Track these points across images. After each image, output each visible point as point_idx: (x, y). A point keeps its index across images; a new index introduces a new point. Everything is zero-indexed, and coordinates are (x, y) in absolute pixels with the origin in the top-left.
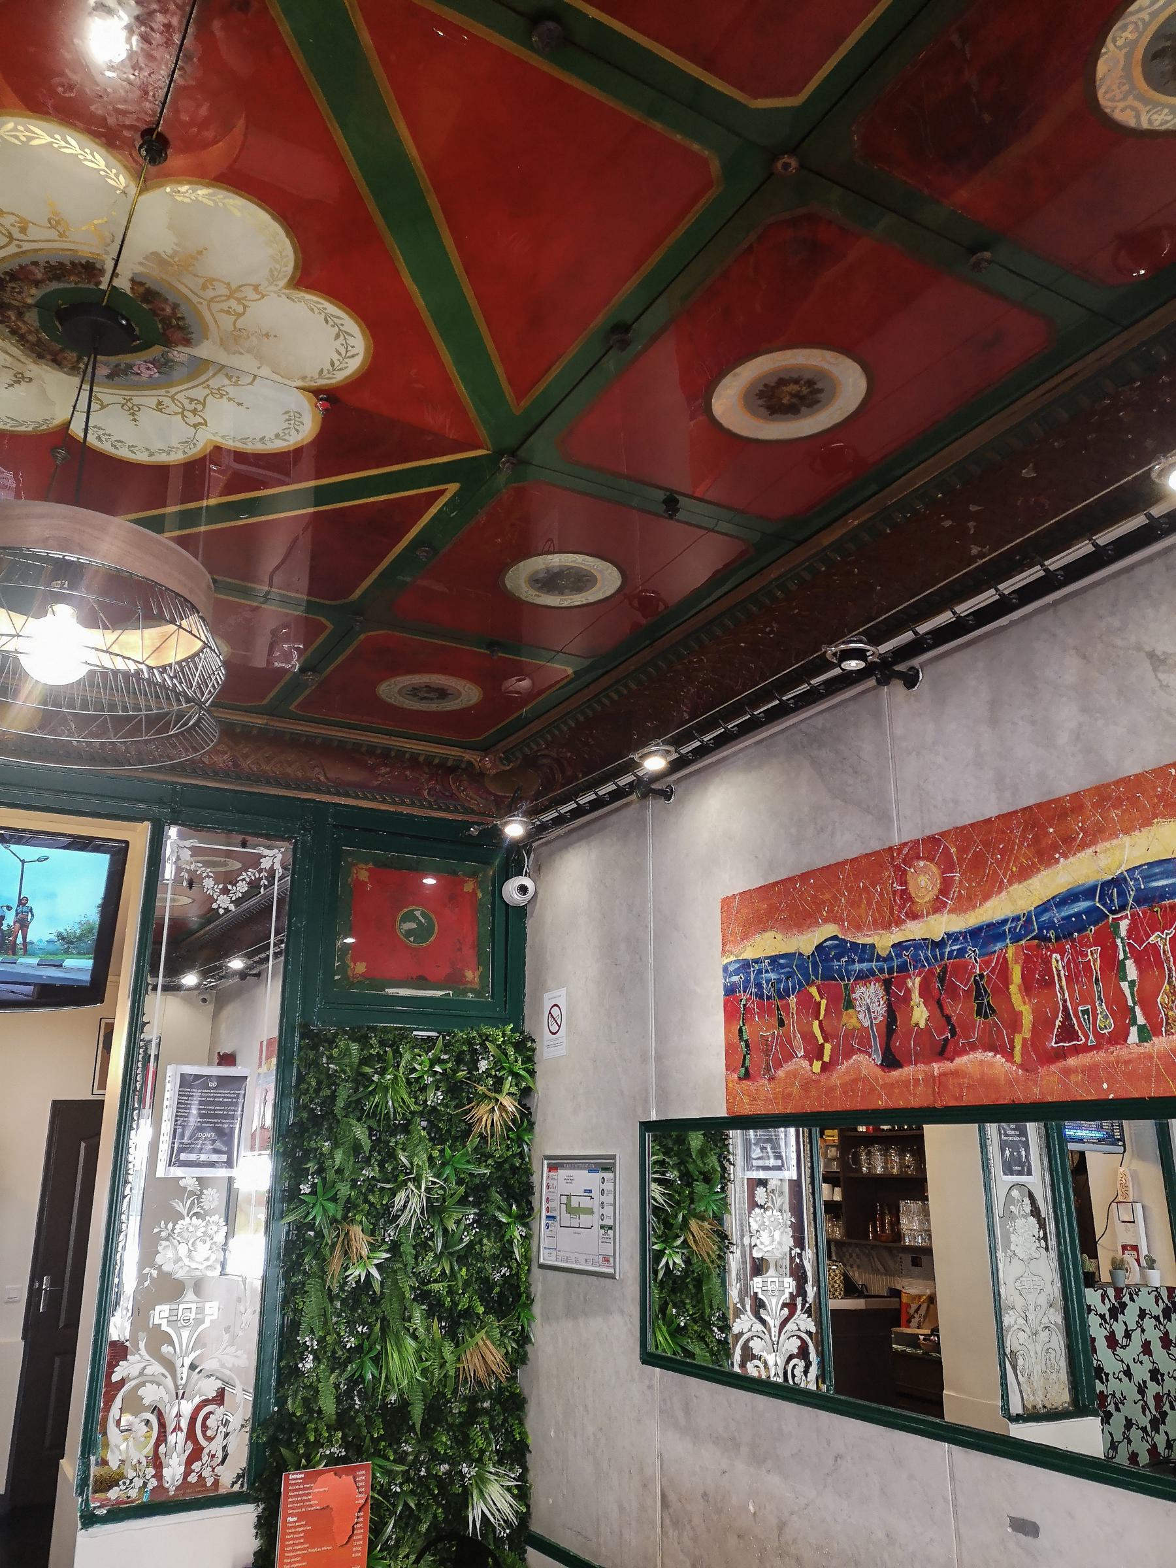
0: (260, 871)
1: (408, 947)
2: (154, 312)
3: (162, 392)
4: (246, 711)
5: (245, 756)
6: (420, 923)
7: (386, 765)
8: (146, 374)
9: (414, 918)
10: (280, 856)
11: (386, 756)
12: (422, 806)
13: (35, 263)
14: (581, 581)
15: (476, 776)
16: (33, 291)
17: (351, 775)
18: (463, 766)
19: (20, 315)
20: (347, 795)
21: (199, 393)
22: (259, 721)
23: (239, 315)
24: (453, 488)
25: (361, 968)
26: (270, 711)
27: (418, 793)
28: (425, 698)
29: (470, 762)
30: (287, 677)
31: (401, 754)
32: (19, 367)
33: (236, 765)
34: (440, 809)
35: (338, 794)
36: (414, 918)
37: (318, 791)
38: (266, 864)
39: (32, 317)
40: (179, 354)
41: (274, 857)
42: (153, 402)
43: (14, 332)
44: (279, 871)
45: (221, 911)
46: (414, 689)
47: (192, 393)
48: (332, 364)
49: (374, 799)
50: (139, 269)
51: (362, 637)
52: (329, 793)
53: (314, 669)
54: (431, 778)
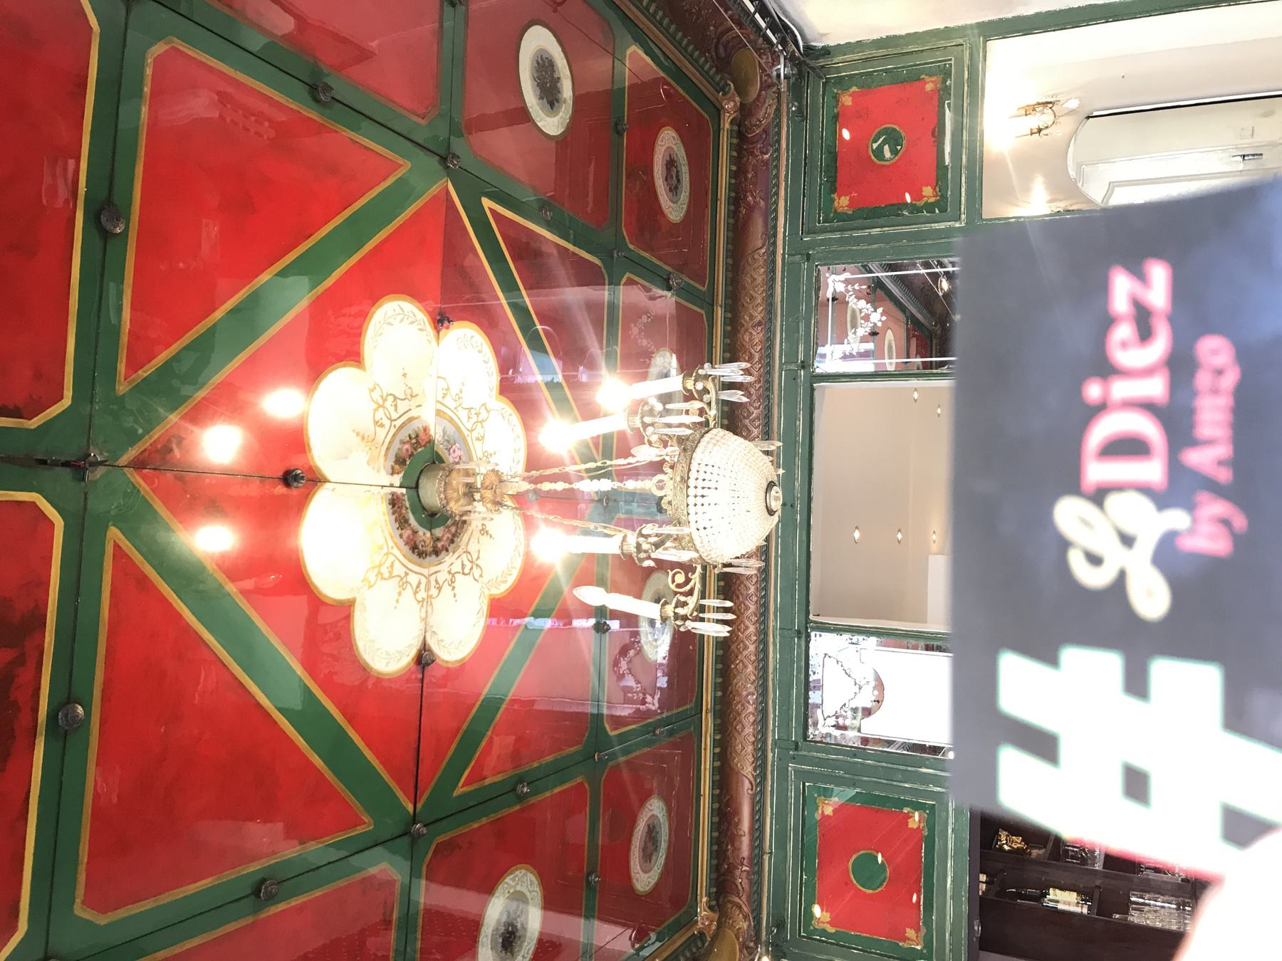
0: (848, 291)
1: (906, 151)
2: (411, 455)
3: (469, 439)
4: (711, 326)
5: (751, 317)
6: (884, 143)
7: (746, 197)
8: (458, 453)
9: (880, 148)
10: (834, 277)
11: (737, 200)
12: (778, 158)
13: (401, 536)
14: (544, 67)
15: (745, 111)
16: (421, 533)
17: (758, 226)
18: (736, 128)
19: (438, 539)
20: (775, 227)
21: (463, 414)
22: (719, 312)
23: (395, 398)
24: (487, 203)
25: (927, 191)
26: (711, 306)
27: (766, 163)
28: (677, 176)
29: (731, 123)
30: (680, 300)
31: (731, 188)
32: (476, 534)
33: (759, 324)
34: (779, 141)
35: (775, 235)
36: (880, 148)
37: (774, 253)
38: (840, 288)
39: (438, 532)
40: (437, 433)
41: (835, 282)
42: (477, 443)
43: (452, 541)
44: (847, 275)
45: (884, 318)
46: (671, 190)
47: (464, 419)
48: (412, 323)
49: (776, 203)
50: (383, 472)
51: (631, 247)
52: (774, 244)
53: (667, 280)
54: (752, 154)
